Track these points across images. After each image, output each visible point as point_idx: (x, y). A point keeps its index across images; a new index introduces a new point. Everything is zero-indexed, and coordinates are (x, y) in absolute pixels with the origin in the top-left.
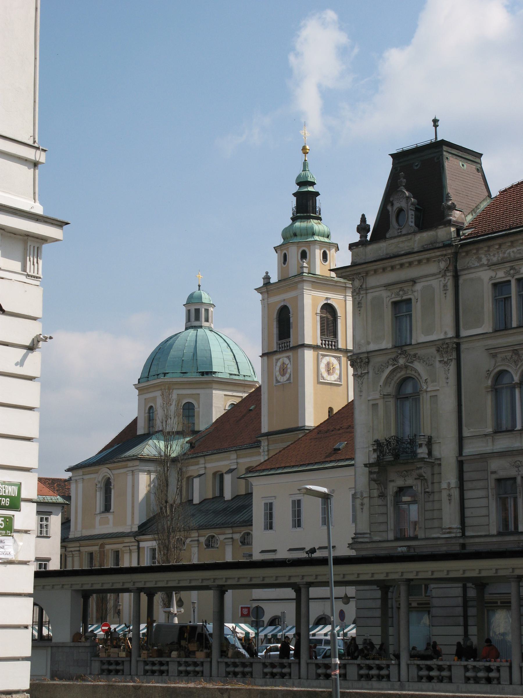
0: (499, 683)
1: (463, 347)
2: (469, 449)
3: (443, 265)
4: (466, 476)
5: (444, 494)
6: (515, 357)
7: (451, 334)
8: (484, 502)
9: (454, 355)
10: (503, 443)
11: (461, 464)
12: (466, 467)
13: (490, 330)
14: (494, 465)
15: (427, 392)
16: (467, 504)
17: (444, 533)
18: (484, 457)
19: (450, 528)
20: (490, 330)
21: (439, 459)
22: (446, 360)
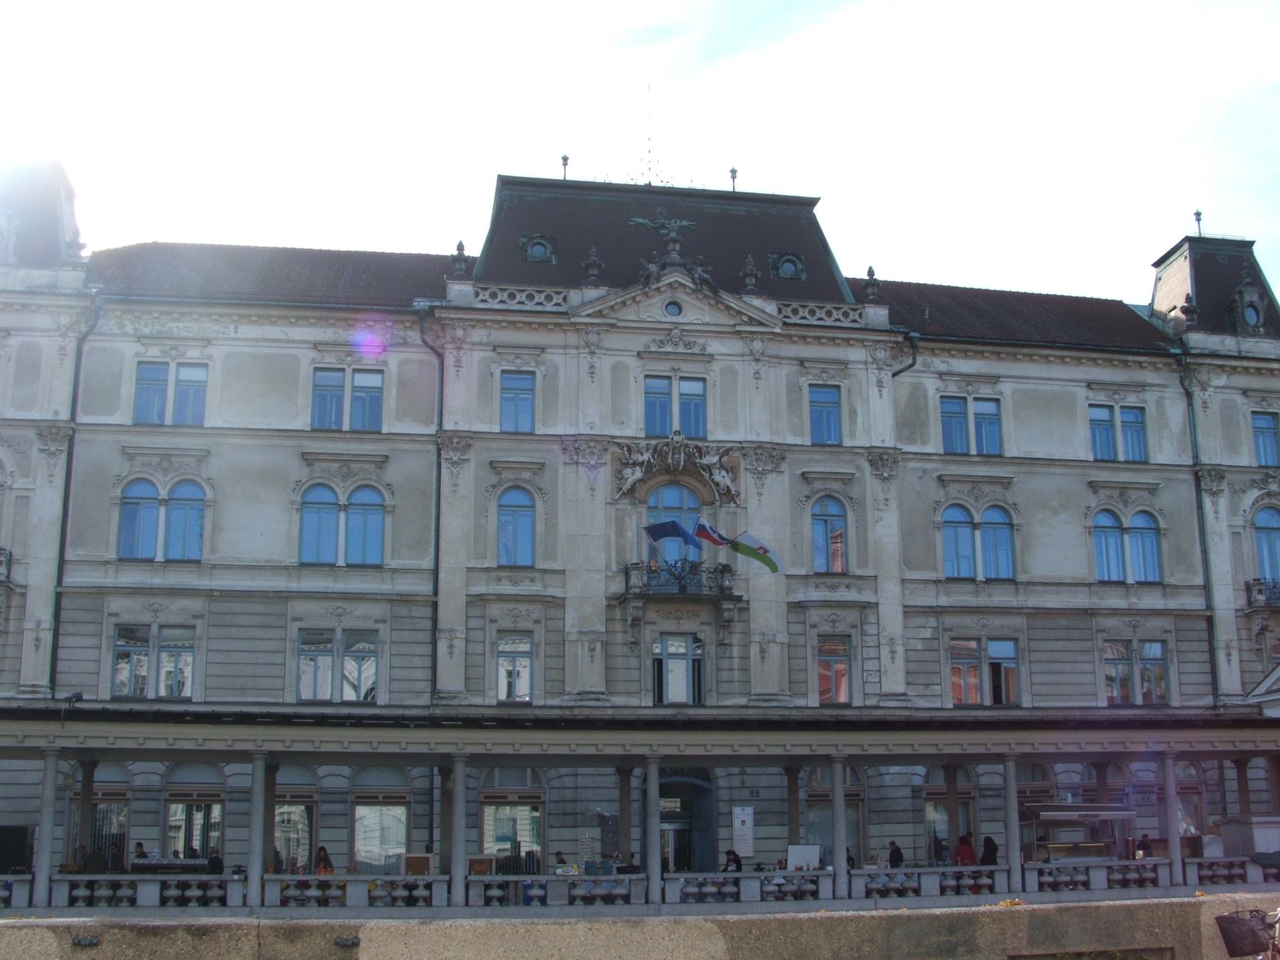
0: (430, 905)
1: (78, 437)
2: (74, 578)
3: (64, 320)
4: (65, 615)
5: (29, 638)
6: (165, 464)
7: (65, 415)
8: (92, 654)
9: (65, 447)
10: (132, 577)
11: (59, 596)
12: (65, 603)
13: (130, 423)
14: (115, 604)
15: (11, 489)
16: (62, 653)
17: (25, 692)
18: (101, 592)
19: (33, 686)
20: (130, 423)
21: (25, 587)
22: (53, 449)
